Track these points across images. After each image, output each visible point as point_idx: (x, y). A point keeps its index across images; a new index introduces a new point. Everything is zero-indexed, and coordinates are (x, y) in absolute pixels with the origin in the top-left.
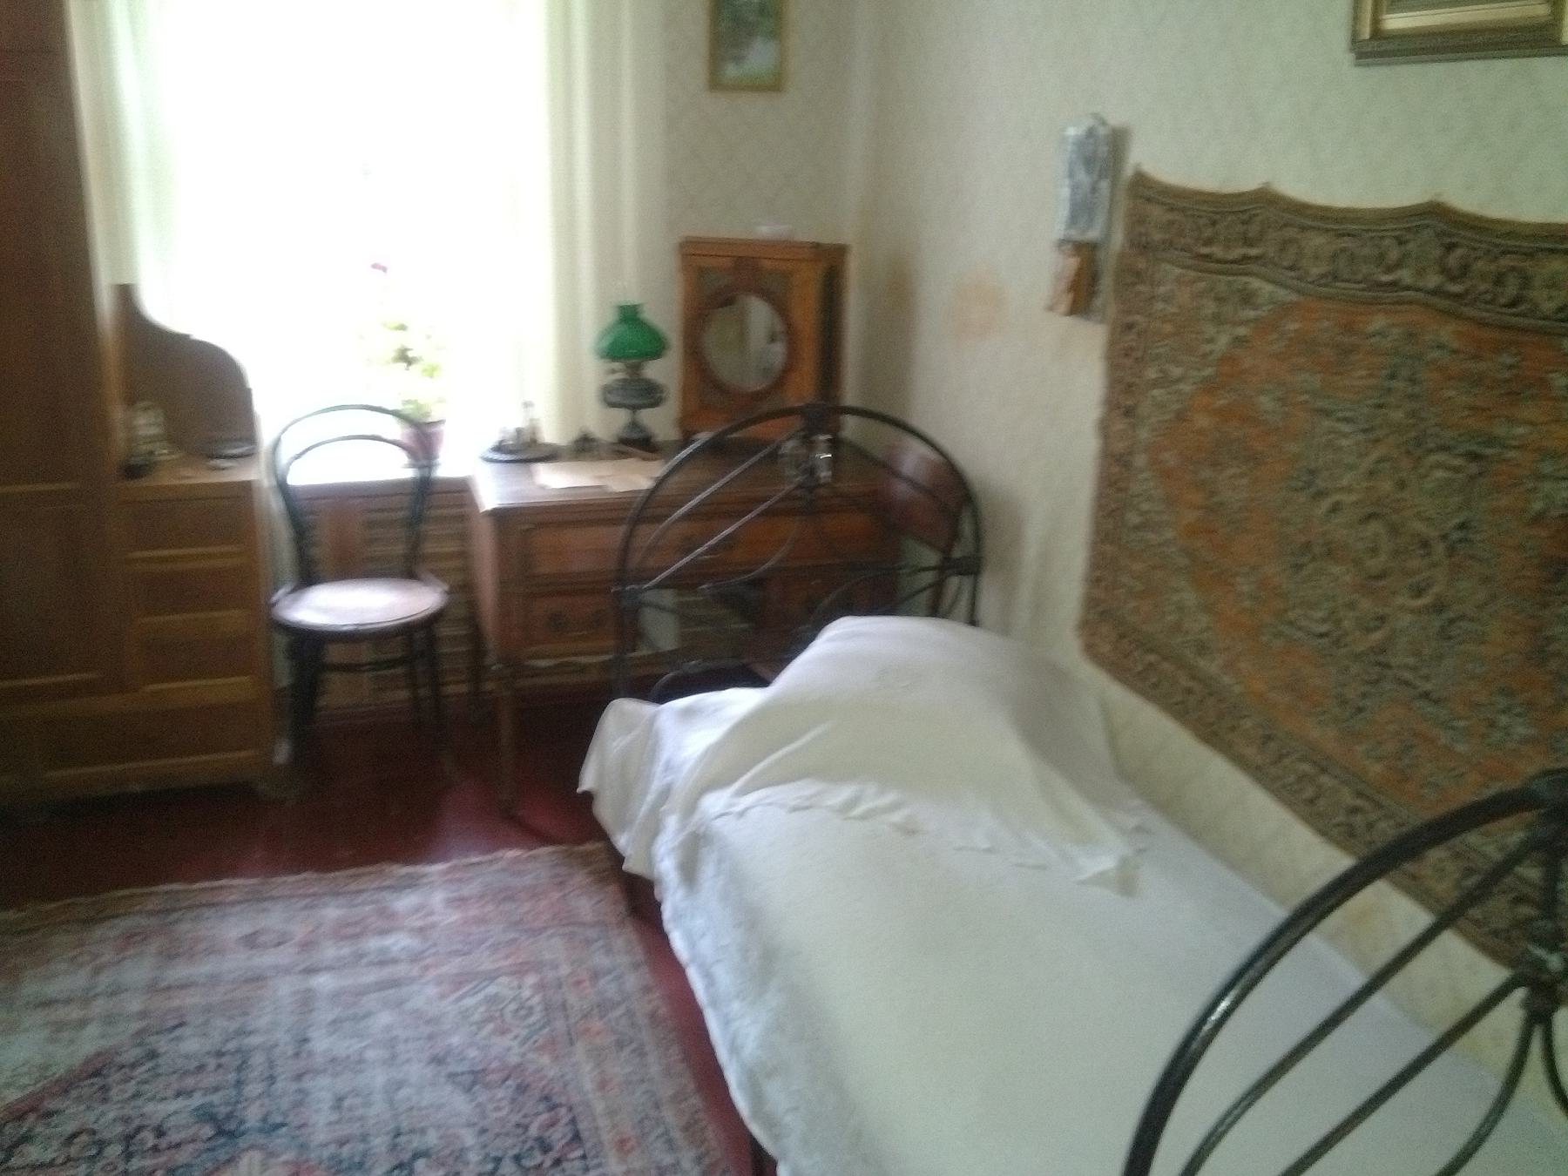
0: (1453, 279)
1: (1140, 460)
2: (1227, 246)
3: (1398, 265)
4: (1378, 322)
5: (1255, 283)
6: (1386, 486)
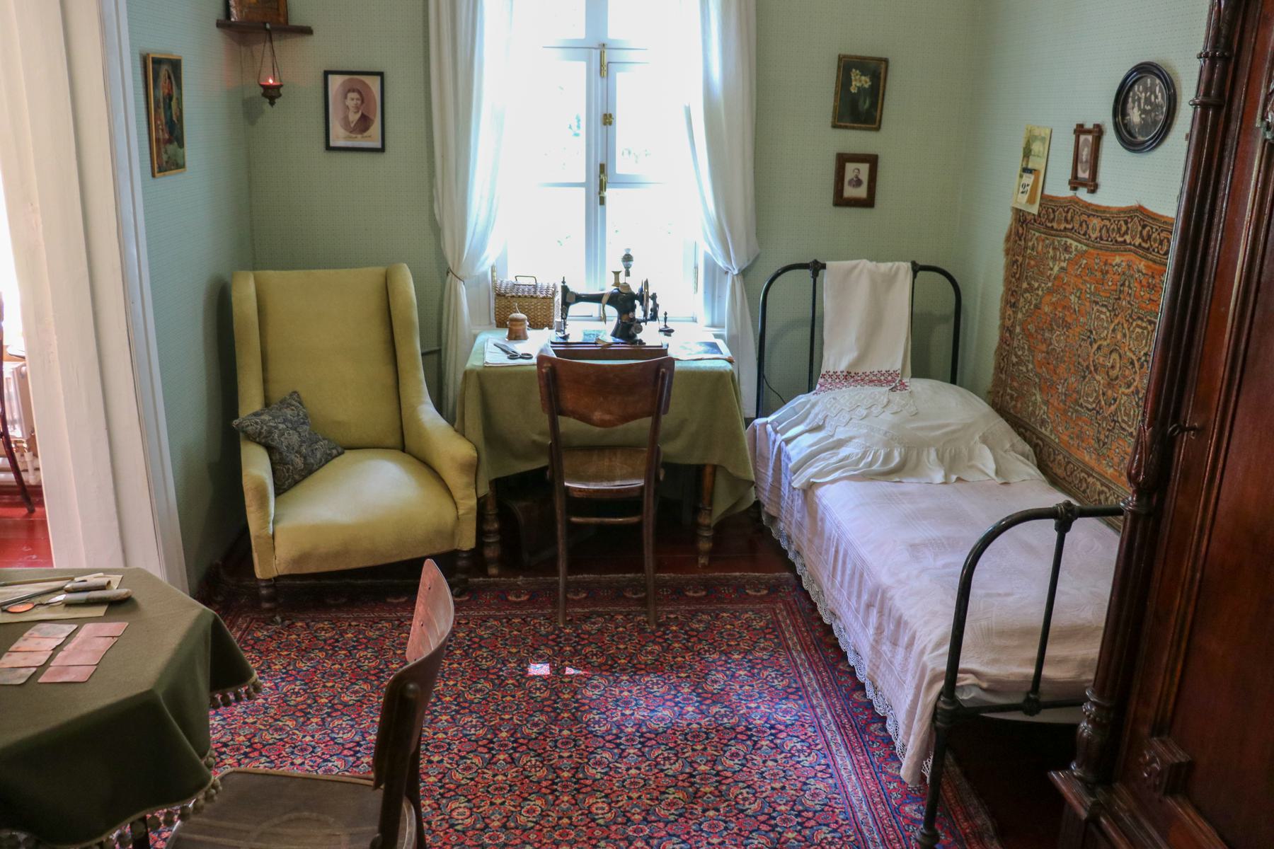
0: (1145, 241)
1: (1018, 329)
2: (1059, 223)
3: (1126, 233)
4: (1118, 260)
5: (1069, 241)
6: (1119, 336)
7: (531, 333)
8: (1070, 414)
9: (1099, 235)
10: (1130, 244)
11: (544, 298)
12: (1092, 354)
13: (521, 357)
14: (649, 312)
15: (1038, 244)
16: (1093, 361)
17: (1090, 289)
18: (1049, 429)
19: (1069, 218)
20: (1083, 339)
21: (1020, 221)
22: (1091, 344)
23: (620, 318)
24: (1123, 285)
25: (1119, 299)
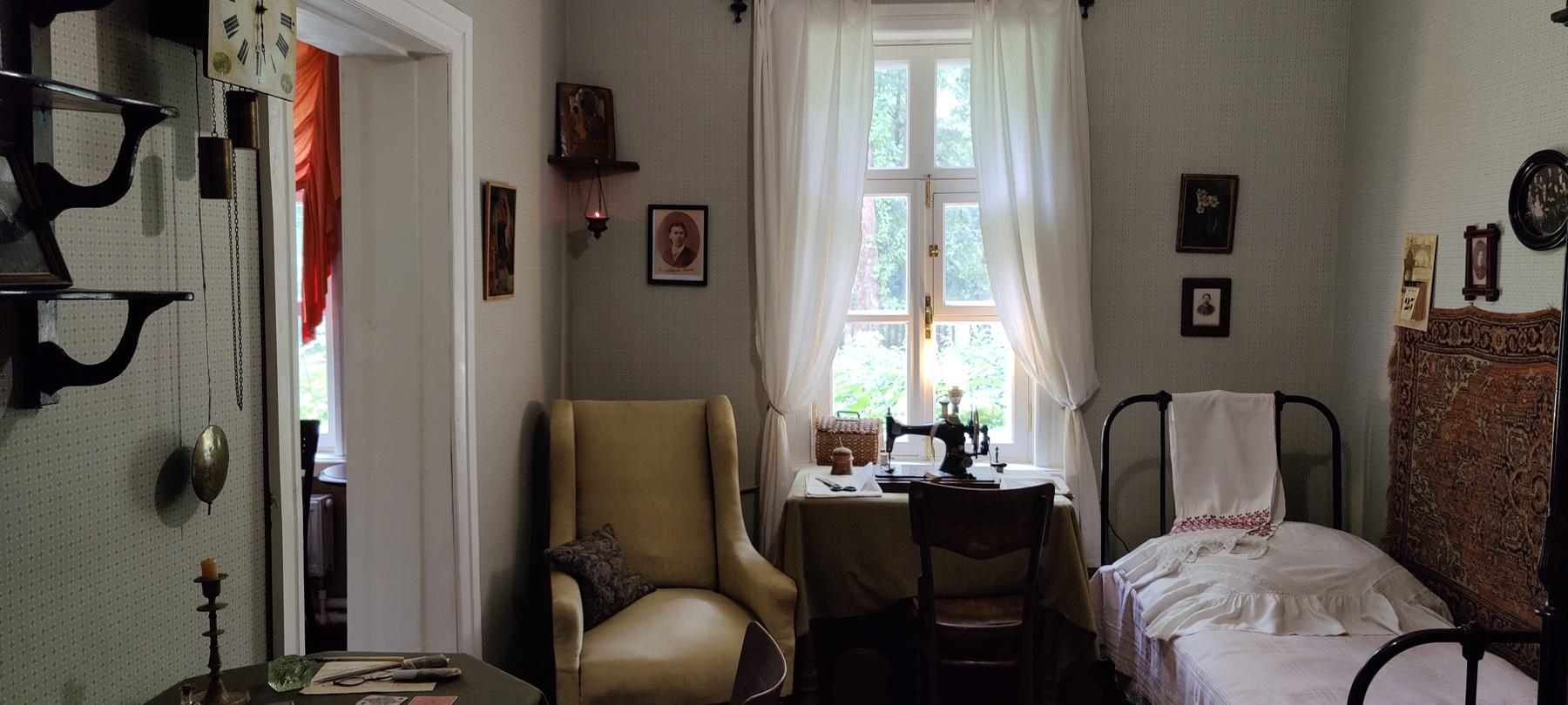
1: (1414, 464)
3: (1539, 341)
4: (1531, 373)
5: (1469, 357)
7: (854, 469)
8: (1490, 558)
9: (1505, 347)
10: (1545, 353)
11: (867, 434)
12: (1510, 485)
13: (844, 490)
14: (980, 446)
15: (1430, 364)
16: (1513, 493)
17: (1500, 409)
18: (1465, 579)
19: (1467, 331)
20: (1497, 468)
21: (1406, 340)
22: (1508, 473)
23: (948, 450)
24: (1541, 400)
25: (1538, 417)
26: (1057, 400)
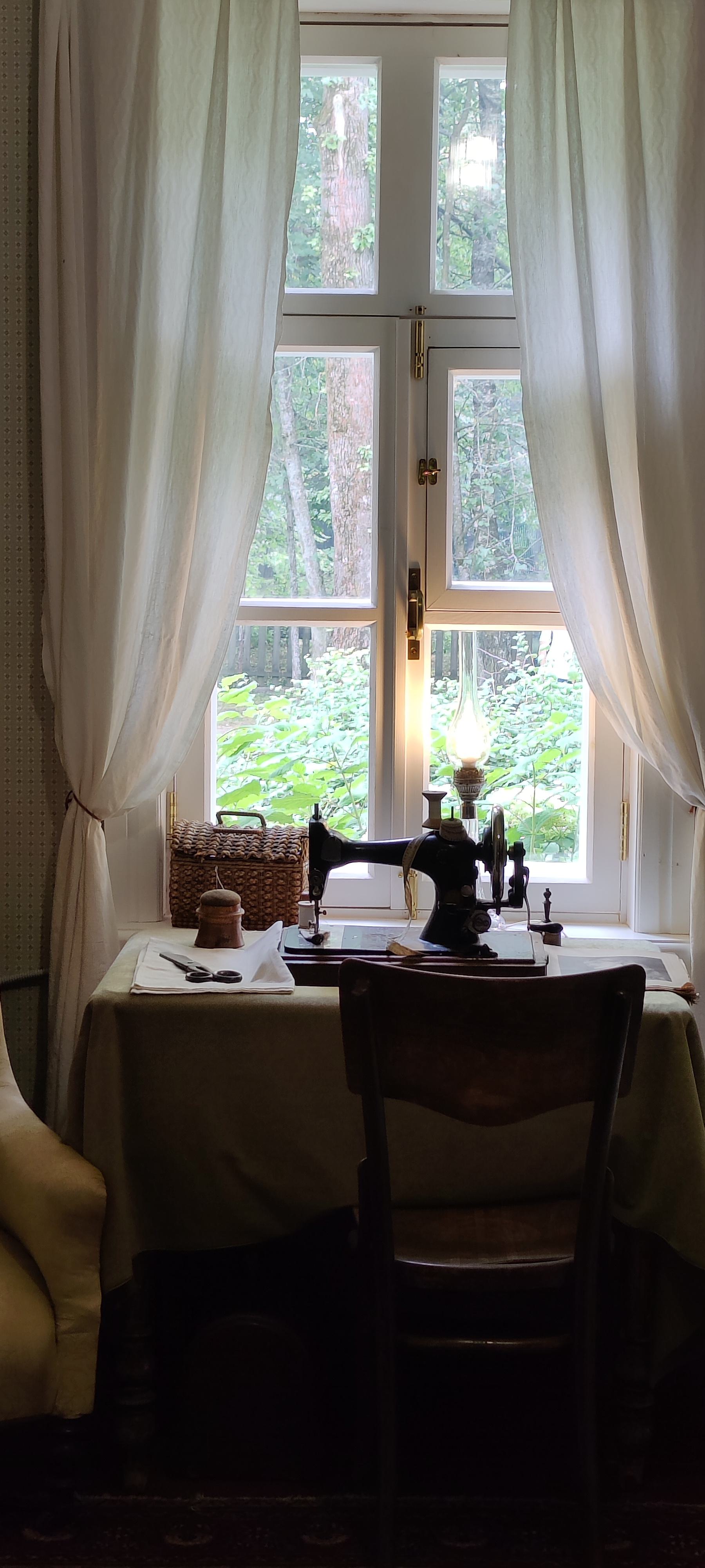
7: (248, 937)
13: (216, 979)
14: (507, 887)
23: (441, 895)
26: (679, 791)
